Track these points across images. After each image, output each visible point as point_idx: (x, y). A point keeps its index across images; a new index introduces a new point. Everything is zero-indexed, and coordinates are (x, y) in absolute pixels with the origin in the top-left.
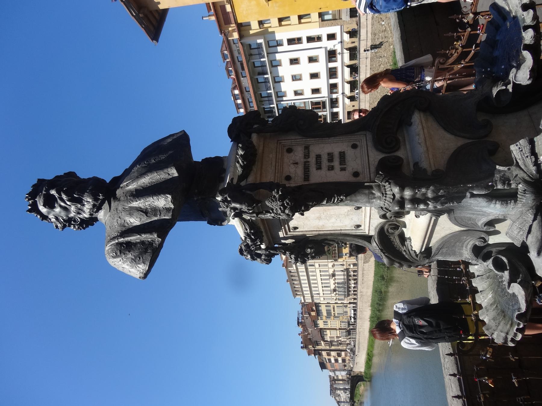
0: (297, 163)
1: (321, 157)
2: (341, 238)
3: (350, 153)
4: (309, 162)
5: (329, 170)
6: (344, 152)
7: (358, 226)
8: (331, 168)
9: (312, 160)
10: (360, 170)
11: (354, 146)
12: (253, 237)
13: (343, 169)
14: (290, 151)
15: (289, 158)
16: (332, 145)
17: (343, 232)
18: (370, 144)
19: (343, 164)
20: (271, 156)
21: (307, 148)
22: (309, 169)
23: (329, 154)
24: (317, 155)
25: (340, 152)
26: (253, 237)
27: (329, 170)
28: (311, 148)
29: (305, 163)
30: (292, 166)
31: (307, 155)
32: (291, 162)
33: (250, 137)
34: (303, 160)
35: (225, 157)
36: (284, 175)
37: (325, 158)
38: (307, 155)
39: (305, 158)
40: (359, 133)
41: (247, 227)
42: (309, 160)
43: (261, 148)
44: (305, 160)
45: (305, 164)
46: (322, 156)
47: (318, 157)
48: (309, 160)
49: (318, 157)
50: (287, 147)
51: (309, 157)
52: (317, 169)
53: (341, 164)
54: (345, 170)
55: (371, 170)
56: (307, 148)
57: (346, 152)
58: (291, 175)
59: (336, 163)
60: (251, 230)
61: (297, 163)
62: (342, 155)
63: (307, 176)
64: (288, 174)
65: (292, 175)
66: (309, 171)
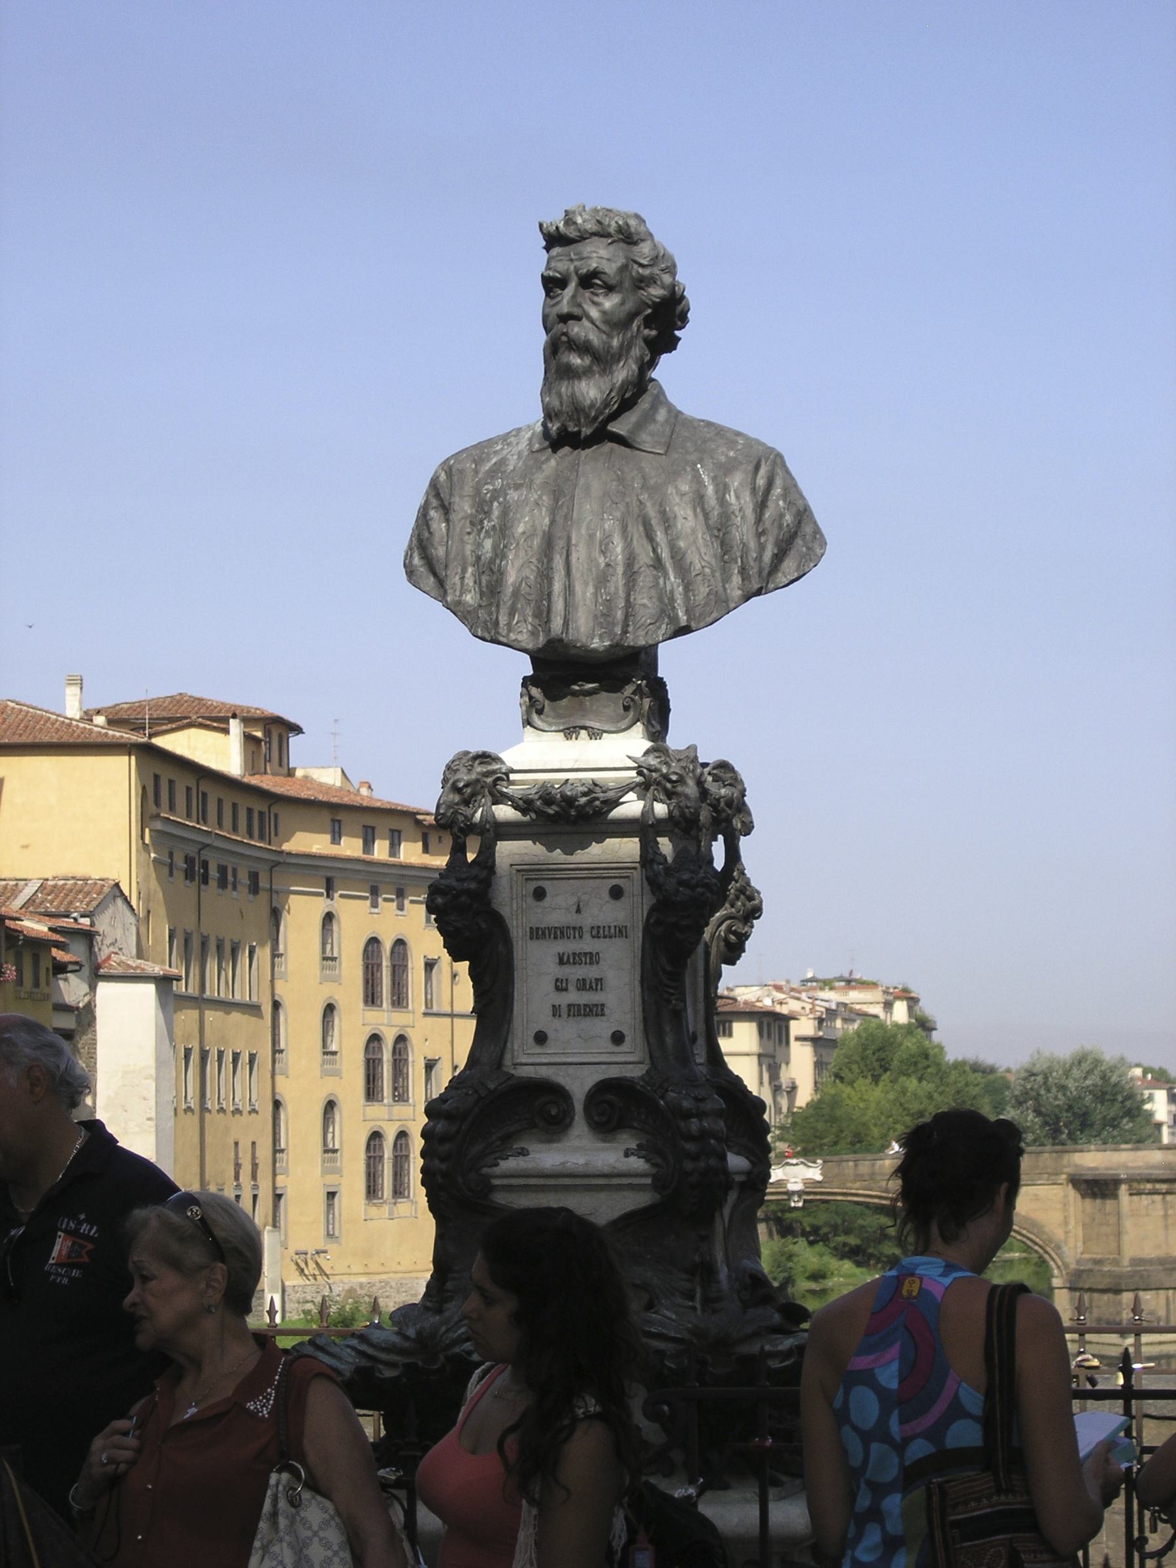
0: (578, 911)
1: (591, 963)
3: (603, 1028)
4: (581, 937)
8: (560, 986)
9: (588, 945)
11: (618, 1038)
13: (556, 1011)
14: (616, 893)
18: (614, 1072)
21: (621, 932)
22: (562, 937)
23: (599, 980)
27: (557, 980)
28: (619, 942)
31: (598, 932)
36: (546, 884)
37: (591, 972)
42: (587, 936)
44: (586, 929)
45: (574, 928)
46: (595, 967)
47: (593, 958)
48: (587, 936)
49: (593, 958)
54: (554, 1015)
56: (621, 932)
58: (548, 899)
59: (573, 996)
61: (578, 911)
62: (595, 1011)
63: (544, 933)
65: (547, 901)
66: (555, 938)
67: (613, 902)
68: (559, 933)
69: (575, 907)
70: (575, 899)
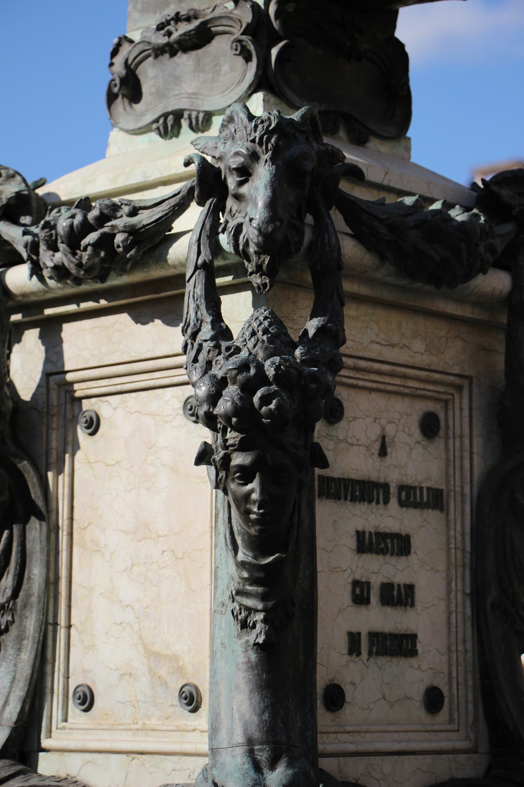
0: (383, 452)
2: (31, 624)
4: (386, 502)
5: (356, 583)
6: (413, 653)
7: (87, 700)
9: (390, 518)
10: (350, 713)
11: (433, 700)
12: (92, 237)
14: (430, 427)
15: (402, 417)
16: (442, 606)
17: (62, 633)
19: (371, 644)
20: (418, 345)
21: (436, 500)
22: (362, 499)
23: (410, 588)
24: (407, 538)
25: (413, 637)
26: (92, 237)
27: (356, 583)
28: (433, 516)
29: (385, 487)
30: (375, 432)
31: (411, 497)
32: (390, 430)
33: (501, 264)
34: (394, 478)
35: (408, 149)
38: (411, 497)
39: (402, 488)
40: (483, 726)
41: (145, 218)
42: (393, 502)
43: (451, 308)
44: (393, 490)
48: (393, 502)
50: (442, 416)
51: (402, 504)
52: (360, 535)
53: (374, 636)
54: (351, 652)
55: (351, 761)
57: (413, 661)
58: (343, 424)
60: (132, 231)
61: (383, 452)
62: (402, 645)
64: (348, 412)
67: (425, 443)
68: (367, 491)
69: (377, 446)
70: (378, 432)
